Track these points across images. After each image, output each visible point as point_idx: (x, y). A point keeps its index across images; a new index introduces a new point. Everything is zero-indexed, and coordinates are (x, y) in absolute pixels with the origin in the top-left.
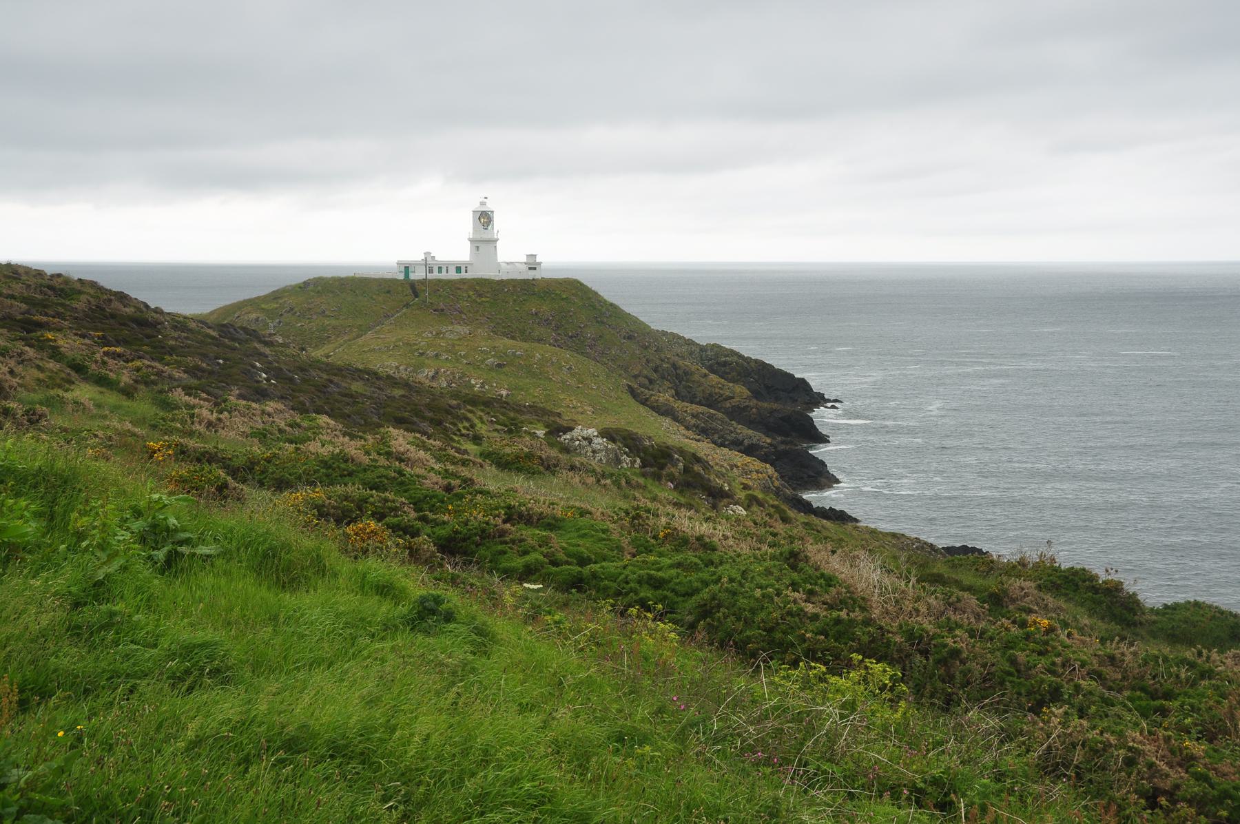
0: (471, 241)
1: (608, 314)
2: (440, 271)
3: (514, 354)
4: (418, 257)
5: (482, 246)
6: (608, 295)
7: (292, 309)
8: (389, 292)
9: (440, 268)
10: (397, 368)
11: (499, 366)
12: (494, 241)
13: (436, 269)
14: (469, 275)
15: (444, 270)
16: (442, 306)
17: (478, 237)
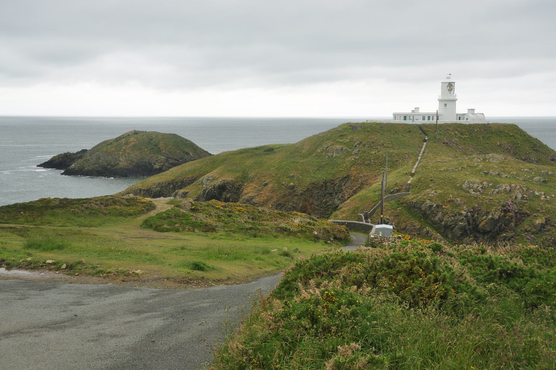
0: (440, 100)
1: (538, 145)
2: (429, 119)
3: (547, 173)
4: (407, 110)
5: (449, 104)
6: (534, 135)
7: (361, 143)
8: (410, 132)
9: (429, 117)
10: (481, 183)
11: (544, 182)
12: (455, 101)
13: (427, 118)
14: (441, 121)
15: (431, 118)
16: (446, 141)
17: (446, 98)
